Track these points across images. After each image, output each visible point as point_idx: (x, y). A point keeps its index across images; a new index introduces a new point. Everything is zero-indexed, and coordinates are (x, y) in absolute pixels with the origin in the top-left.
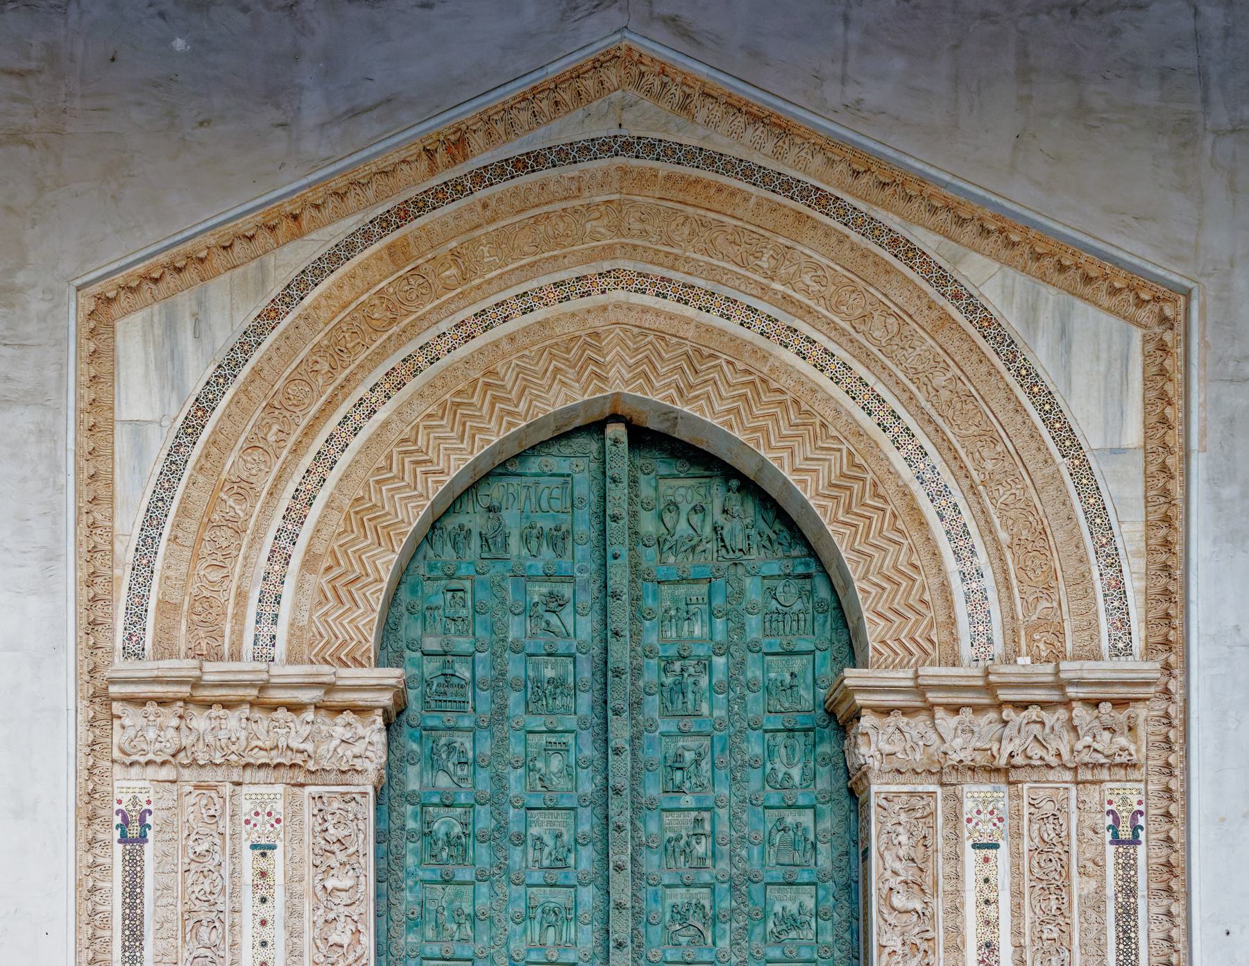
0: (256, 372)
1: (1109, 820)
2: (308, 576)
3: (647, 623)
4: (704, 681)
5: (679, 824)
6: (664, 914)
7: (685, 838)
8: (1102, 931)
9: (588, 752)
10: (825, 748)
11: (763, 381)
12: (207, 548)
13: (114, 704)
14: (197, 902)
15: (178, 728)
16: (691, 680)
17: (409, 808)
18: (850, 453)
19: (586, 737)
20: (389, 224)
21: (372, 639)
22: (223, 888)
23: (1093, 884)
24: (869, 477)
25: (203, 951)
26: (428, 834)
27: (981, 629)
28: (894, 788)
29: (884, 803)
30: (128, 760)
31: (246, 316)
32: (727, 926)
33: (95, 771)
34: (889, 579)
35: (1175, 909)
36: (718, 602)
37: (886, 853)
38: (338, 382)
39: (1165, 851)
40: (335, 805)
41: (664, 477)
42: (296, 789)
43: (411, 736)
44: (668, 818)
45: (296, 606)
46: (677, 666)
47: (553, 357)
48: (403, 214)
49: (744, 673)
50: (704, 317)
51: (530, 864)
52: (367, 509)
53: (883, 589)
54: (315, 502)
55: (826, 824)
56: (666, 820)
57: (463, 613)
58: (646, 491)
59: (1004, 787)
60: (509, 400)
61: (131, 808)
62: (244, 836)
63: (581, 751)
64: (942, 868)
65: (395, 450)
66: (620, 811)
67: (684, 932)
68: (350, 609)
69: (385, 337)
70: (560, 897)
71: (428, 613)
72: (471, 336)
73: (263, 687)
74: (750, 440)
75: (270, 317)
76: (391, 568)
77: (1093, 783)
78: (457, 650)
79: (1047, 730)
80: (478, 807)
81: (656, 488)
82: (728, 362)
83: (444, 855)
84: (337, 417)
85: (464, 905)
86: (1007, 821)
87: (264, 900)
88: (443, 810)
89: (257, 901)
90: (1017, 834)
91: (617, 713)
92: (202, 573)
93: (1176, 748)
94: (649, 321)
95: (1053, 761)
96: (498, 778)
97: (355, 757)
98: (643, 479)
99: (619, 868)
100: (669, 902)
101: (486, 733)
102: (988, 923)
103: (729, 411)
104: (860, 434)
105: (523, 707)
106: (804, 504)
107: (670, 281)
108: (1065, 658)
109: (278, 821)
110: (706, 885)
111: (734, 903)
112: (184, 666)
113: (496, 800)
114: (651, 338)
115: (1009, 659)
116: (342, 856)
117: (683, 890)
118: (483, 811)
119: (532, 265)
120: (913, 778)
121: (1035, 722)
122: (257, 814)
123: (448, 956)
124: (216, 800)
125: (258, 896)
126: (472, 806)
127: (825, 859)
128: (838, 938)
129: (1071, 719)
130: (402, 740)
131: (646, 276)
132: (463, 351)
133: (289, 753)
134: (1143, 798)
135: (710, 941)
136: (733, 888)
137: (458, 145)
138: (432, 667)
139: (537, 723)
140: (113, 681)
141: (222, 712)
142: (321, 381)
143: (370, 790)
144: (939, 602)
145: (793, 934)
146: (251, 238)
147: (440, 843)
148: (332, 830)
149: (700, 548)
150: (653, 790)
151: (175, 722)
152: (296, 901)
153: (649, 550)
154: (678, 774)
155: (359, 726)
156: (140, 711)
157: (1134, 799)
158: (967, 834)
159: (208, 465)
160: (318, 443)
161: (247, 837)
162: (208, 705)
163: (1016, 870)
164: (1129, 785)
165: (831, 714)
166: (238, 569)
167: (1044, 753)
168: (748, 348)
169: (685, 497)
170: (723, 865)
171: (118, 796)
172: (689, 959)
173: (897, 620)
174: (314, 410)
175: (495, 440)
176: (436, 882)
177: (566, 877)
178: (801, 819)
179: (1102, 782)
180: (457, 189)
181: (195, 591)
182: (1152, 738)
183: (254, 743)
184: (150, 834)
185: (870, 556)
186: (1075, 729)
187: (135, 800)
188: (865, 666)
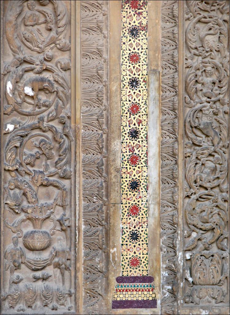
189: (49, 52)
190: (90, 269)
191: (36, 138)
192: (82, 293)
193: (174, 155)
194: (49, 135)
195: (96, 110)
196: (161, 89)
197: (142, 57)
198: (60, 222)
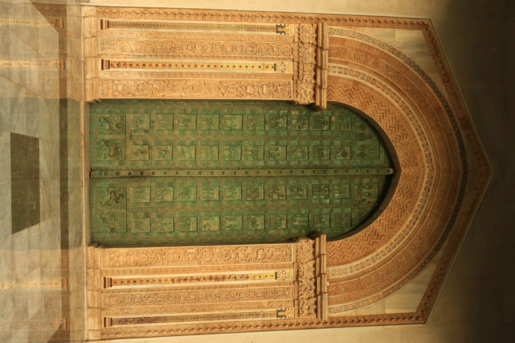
0: (408, 69)
1: (283, 309)
2: (352, 82)
3: (339, 181)
4: (322, 197)
5: (282, 190)
6: (256, 186)
7: (278, 192)
8: (252, 309)
9: (303, 164)
11: (404, 211)
12: (360, 53)
13: (316, 25)
14: (259, 48)
15: (309, 43)
16: (323, 193)
17: (286, 112)
18: (384, 235)
19: (307, 163)
20: (446, 107)
21: (334, 100)
22: (263, 55)
23: (266, 305)
24: (378, 241)
25: (244, 49)
26: (279, 117)
27: (337, 272)
28: (292, 250)
29: (288, 247)
30: (300, 28)
31: (423, 67)
32: (252, 204)
33: (297, 19)
34: (351, 247)
35: (259, 327)
36: (344, 200)
37: (274, 248)
38: (405, 92)
39: (275, 324)
40: (287, 89)
41: (378, 185)
44: (283, 187)
45: (344, 79)
46: (327, 189)
47: (411, 153)
48: (449, 111)
49: (325, 208)
50: (421, 194)
51: (270, 147)
52: (371, 100)
53: (348, 245)
54: (372, 85)
55: (282, 232)
56: (283, 186)
57: (342, 128)
58: (375, 180)
59: (293, 280)
60: (400, 141)
61: (286, 29)
62: (278, 62)
64: (271, 264)
65: (386, 108)
66: (285, 173)
68: (343, 94)
69: (417, 105)
71: (342, 118)
72: (417, 130)
73: (321, 68)
74: (389, 208)
75: (423, 73)
76: (354, 106)
77: (294, 304)
78: (331, 126)
79: (309, 291)
80: (287, 131)
81: (375, 183)
82: (409, 201)
83: (273, 122)
84: (395, 92)
85: (258, 127)
86: (283, 281)
87: (259, 67)
88: (286, 121)
89: (259, 65)
90: (279, 284)
91: (314, 172)
92: (353, 52)
93: (304, 326)
94: (420, 179)
95: (300, 293)
96: (295, 138)
97: (301, 95)
98: (378, 179)
99: (269, 172)
100: (259, 187)
101: (308, 134)
102: (254, 277)
103: (396, 202)
104: (390, 238)
106: (371, 223)
107: (431, 185)
108: (328, 296)
109: (283, 72)
111: (259, 206)
112: (327, 45)
113: (289, 137)
114: (416, 180)
115: (328, 280)
116: (272, 90)
117: (263, 191)
118: (286, 133)
119: (435, 147)
120: (295, 255)
121: (311, 288)
122: (285, 66)
123: (243, 122)
124: (289, 54)
125: (261, 65)
126: (287, 130)
127: (272, 232)
128: (250, 236)
129: (312, 297)
130: (306, 110)
131: (432, 179)
132: (413, 127)
133: (302, 75)
134: (290, 318)
135: (248, 199)
136: (264, 206)
137: (467, 126)
138: (327, 119)
139: (311, 149)
140: (322, 24)
141: (314, 56)
142: (405, 87)
143: (292, 99)
144: (344, 261)
145: (250, 223)
146: (443, 69)
147: (276, 120)
148: (280, 87)
149: (359, 196)
150: (292, 182)
151: (311, 42)
152: (259, 77)
153: (359, 181)
154: (296, 190)
155: (310, 96)
156: (314, 32)
157: (289, 316)
158: (279, 270)
159: (383, 55)
160: (389, 86)
161: (278, 63)
162: (316, 52)
163: (269, 284)
164: (293, 314)
165: (313, 232)
166: (354, 62)
167: (302, 291)
168: (413, 207)
169: (373, 191)
170: (270, 203)
171: (290, 25)
172: (243, 193)
173: (339, 249)
174: (397, 85)
175: (389, 137)
176: (265, 119)
177: (266, 157)
178: (283, 225)
179: (294, 307)
180: (455, 127)
181: (348, 50)
182: (306, 320)
183: (305, 65)
184: (279, 34)
185: (357, 242)
186: (309, 299)
188: (326, 241)
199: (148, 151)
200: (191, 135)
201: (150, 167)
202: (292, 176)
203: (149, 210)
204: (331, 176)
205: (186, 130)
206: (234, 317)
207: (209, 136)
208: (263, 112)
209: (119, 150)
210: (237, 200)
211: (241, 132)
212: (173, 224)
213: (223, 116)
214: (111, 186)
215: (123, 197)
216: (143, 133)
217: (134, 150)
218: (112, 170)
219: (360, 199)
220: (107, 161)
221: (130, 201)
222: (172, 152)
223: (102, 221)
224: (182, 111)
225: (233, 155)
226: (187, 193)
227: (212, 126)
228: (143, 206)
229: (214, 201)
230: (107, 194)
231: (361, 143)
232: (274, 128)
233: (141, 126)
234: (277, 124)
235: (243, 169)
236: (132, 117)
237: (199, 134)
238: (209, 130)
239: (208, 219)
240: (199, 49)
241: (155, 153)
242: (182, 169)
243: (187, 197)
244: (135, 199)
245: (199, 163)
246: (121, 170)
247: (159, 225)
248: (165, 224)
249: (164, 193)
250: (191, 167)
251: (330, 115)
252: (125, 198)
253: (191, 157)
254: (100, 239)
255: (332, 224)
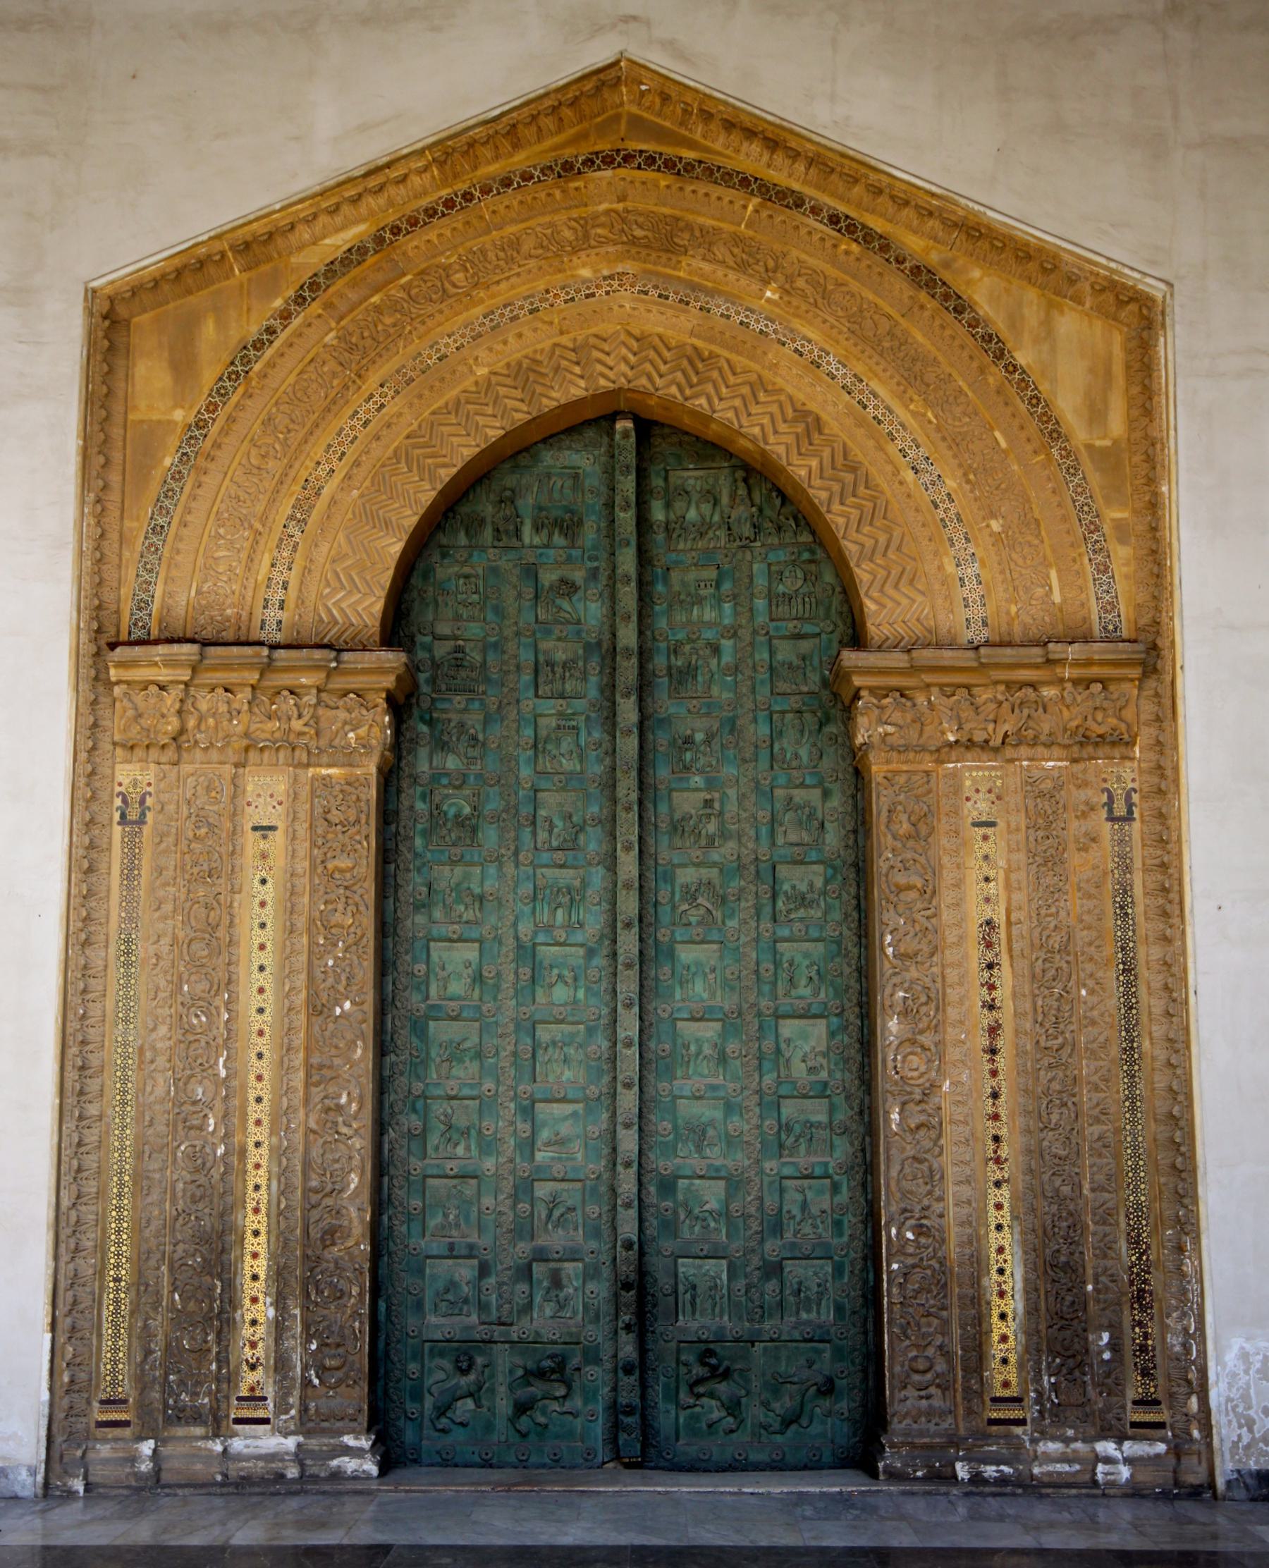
6: (673, 893)
9: (596, 735)
10: (831, 729)
17: (419, 789)
26: (436, 814)
36: (727, 586)
42: (299, 771)
43: (422, 719)
49: (752, 655)
55: (835, 802)
63: (589, 733)
67: (693, 911)
70: (567, 877)
81: (666, 479)
105: (531, 693)
110: (714, 864)
125: (258, 877)
127: (833, 838)
128: (846, 915)
130: (411, 722)
145: (801, 913)
147: (449, 825)
148: (334, 812)
187: (135, 783)
189: (926, 1202)
190: (967, 1389)
191: (917, 1276)
192: (961, 1411)
193: (1037, 1290)
194: (929, 1272)
195: (968, 1251)
196: (1022, 1233)
197: (1006, 1205)
198: (940, 1347)
199: (553, 1265)
200: (498, 1116)
201: (605, 1258)
202: (641, 770)
203: (756, 1261)
204: (641, 633)
205: (480, 1132)
206: (1130, 971)
207: (503, 1054)
208: (419, 871)
209: (547, 1363)
210: (721, 958)
211: (487, 945)
212: (806, 1182)
213: (433, 1007)
214: (672, 1395)
215: (711, 1353)
216: (491, 1281)
217: (548, 1312)
218: (614, 1389)
219: (722, 533)
220: (585, 1404)
221: (724, 1328)
222: (555, 1180)
223: (794, 1427)
224: (415, 1146)
225: (566, 973)
226: (699, 1134)
227: (467, 1045)
228: (741, 1283)
229: (724, 1035)
230: (698, 1409)
231: (527, 530)
232: (474, 830)
233: (466, 1289)
234: (460, 821)
235: (615, 941)
236: (432, 1319)
237: (492, 1086)
238: (479, 1055)
239: (788, 1061)
240: (200, 1091)
241: (555, 1240)
242: (614, 1149)
243: (711, 1132)
244: (717, 1310)
245: (593, 1090)
246: (615, 1356)
247: (807, 1229)
248: (804, 1206)
249: (696, 1211)
250: (605, 1116)
251: (428, 639)
252: (712, 1346)
253: (574, 1114)
254: (855, 1435)
255: (808, 628)
